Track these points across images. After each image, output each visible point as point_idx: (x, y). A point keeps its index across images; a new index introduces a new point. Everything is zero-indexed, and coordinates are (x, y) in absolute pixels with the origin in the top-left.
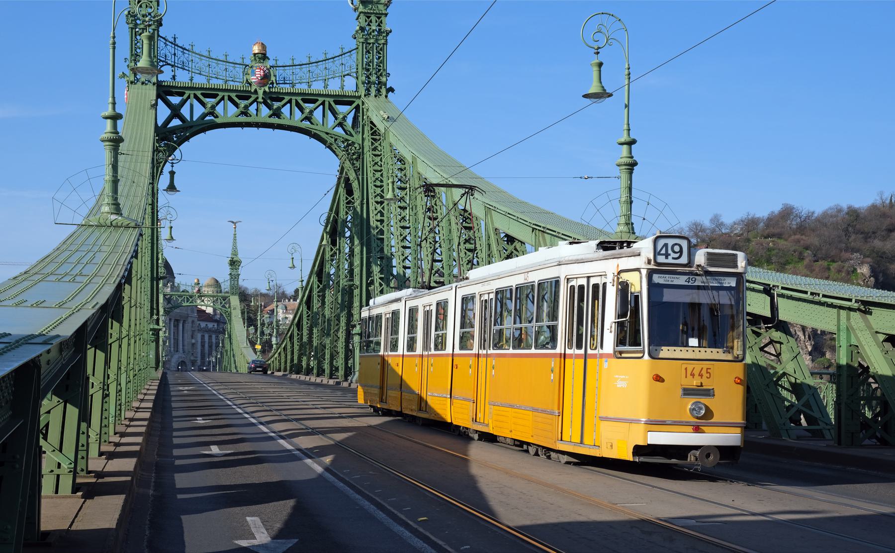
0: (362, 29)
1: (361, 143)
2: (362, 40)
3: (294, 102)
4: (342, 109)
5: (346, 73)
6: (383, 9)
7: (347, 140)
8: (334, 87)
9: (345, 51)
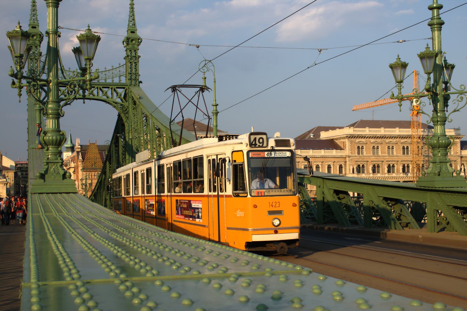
0: (128, 56)
1: (128, 106)
2: (128, 61)
3: (99, 88)
4: (120, 91)
5: (122, 75)
6: (136, 47)
7: (122, 105)
8: (116, 80)
9: (121, 65)
